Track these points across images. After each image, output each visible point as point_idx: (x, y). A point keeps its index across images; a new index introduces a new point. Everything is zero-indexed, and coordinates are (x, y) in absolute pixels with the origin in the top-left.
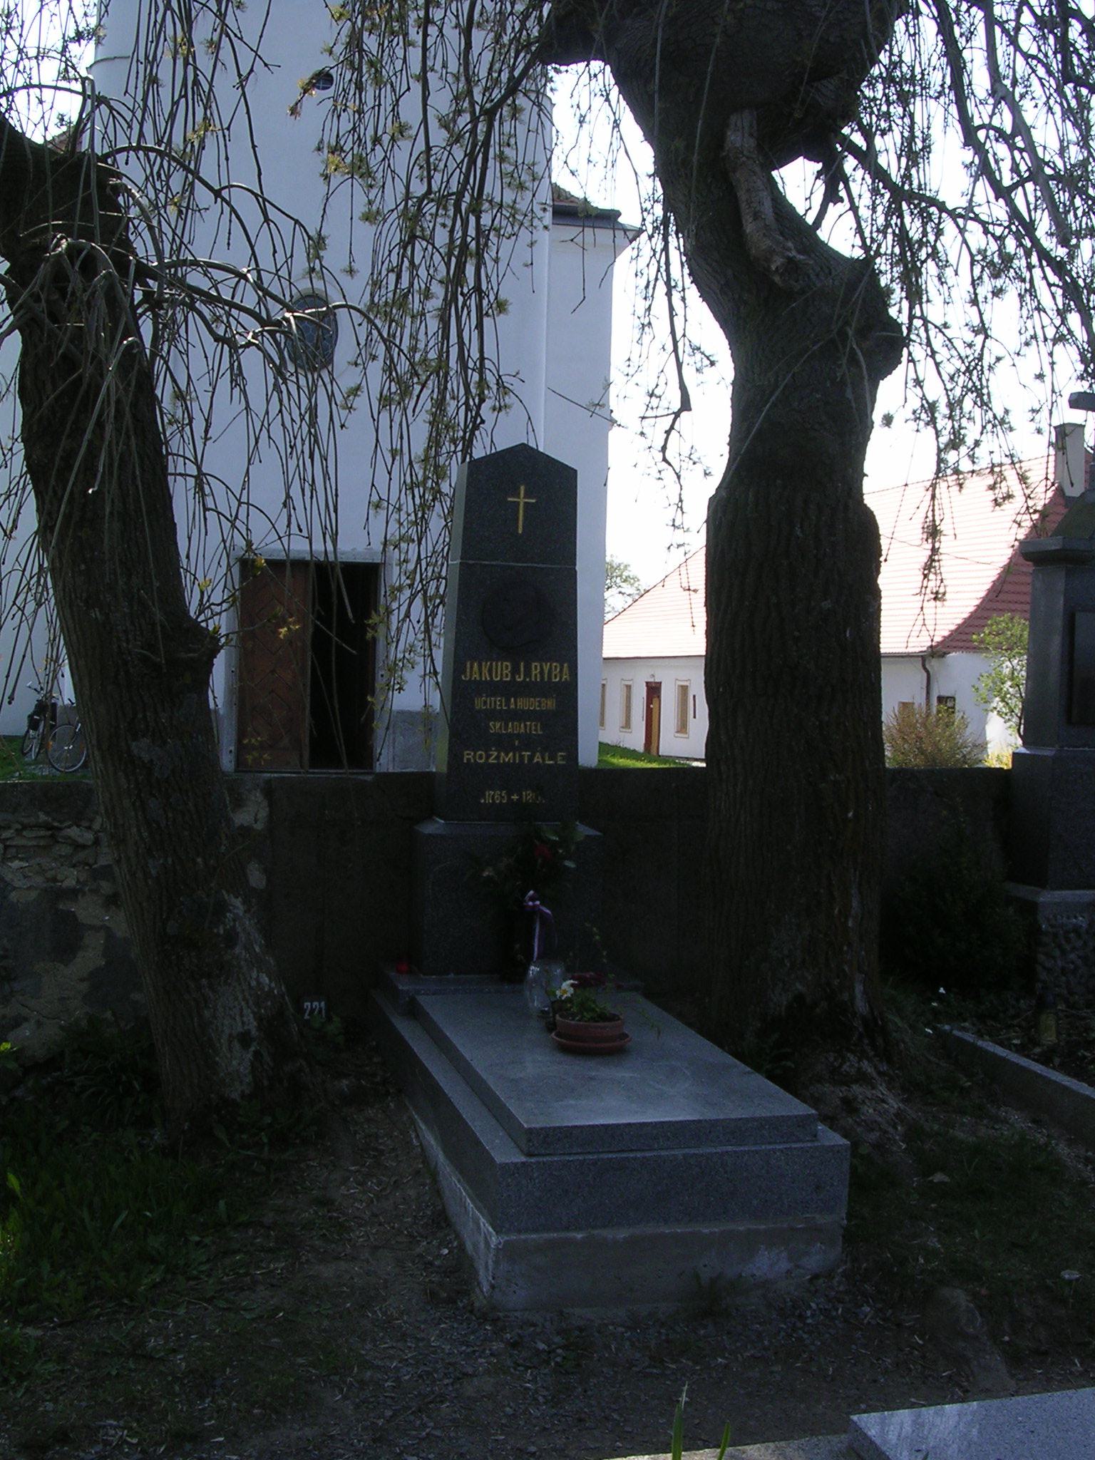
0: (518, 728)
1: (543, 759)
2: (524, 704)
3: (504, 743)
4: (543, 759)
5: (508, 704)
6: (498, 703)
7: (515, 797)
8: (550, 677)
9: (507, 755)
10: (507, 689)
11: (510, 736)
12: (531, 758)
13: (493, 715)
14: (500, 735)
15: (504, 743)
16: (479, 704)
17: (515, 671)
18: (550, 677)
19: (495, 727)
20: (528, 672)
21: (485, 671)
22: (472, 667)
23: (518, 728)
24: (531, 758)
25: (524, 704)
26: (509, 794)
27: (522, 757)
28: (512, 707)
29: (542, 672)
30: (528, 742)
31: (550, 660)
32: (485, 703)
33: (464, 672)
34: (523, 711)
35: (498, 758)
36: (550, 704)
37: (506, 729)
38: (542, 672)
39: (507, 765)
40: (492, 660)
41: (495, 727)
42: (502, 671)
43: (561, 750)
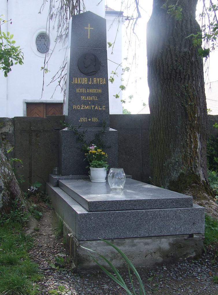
1: (98, 108)
2: (91, 91)
3: (86, 103)
4: (98, 108)
5: (87, 91)
6: (83, 90)
7: (90, 120)
8: (99, 82)
9: (87, 106)
10: (87, 87)
12: (94, 107)
13: (81, 94)
14: (85, 100)
15: (86, 103)
16: (77, 91)
17: (89, 81)
18: (99, 82)
19: (83, 98)
20: (92, 81)
21: (79, 81)
22: (75, 79)
24: (94, 107)
25: (91, 91)
26: (88, 119)
27: (91, 107)
28: (88, 92)
29: (97, 81)
30: (93, 103)
32: (79, 90)
33: (73, 81)
34: (92, 93)
35: (84, 107)
36: (100, 91)
37: (86, 98)
38: (97, 81)
40: (81, 77)
41: (83, 98)
42: (84, 80)
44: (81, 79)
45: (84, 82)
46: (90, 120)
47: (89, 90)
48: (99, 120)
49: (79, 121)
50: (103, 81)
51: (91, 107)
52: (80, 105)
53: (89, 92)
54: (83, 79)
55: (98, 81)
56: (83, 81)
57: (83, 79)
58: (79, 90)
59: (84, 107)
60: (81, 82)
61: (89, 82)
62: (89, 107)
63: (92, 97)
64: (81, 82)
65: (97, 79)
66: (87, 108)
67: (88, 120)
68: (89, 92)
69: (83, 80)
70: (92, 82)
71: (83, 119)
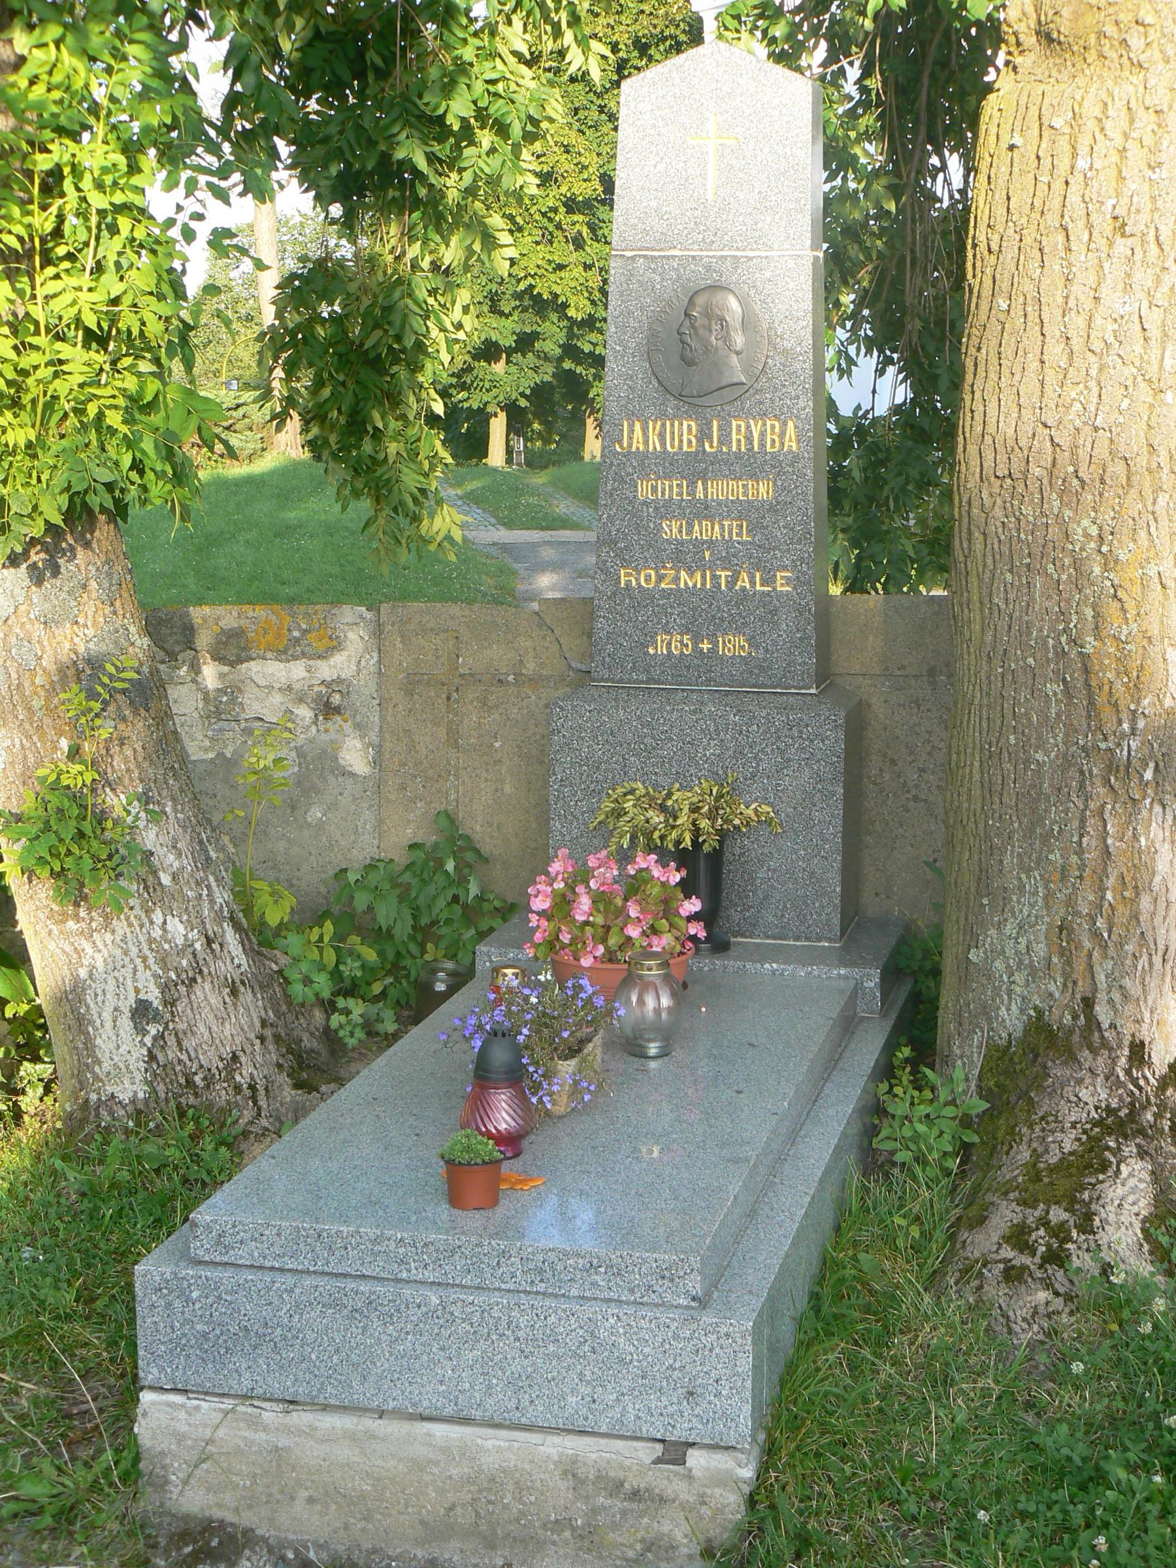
0: (703, 531)
1: (753, 583)
2: (719, 490)
3: (686, 555)
4: (753, 583)
5: (692, 493)
6: (673, 489)
7: (705, 646)
8: (762, 445)
10: (696, 467)
11: (698, 543)
13: (666, 509)
14: (682, 543)
16: (644, 490)
17: (704, 435)
18: (762, 445)
19: (671, 529)
20: (725, 439)
21: (654, 440)
22: (631, 431)
23: (703, 531)
25: (719, 490)
26: (697, 639)
27: (715, 577)
28: (700, 494)
30: (728, 557)
31: (764, 415)
32: (654, 489)
33: (620, 442)
34: (719, 504)
36: (764, 490)
38: (749, 439)
39: (692, 592)
40: (662, 416)
42: (683, 434)
43: (785, 568)
44: (664, 425)
45: (681, 441)
46: (705, 646)
47: (705, 489)
48: (757, 647)
49: (651, 651)
50: (782, 435)
51: (715, 577)
52: (657, 570)
53: (706, 496)
54: (672, 425)
55: (756, 435)
56: (673, 439)
57: (672, 425)
58: (654, 489)
59: (677, 579)
60: (663, 444)
61: (707, 445)
62: (704, 577)
63: (722, 527)
64: (663, 444)
65: (748, 427)
66: (690, 584)
67: (695, 644)
68: (706, 496)
69: (673, 433)
70: (721, 443)
71: (669, 644)
